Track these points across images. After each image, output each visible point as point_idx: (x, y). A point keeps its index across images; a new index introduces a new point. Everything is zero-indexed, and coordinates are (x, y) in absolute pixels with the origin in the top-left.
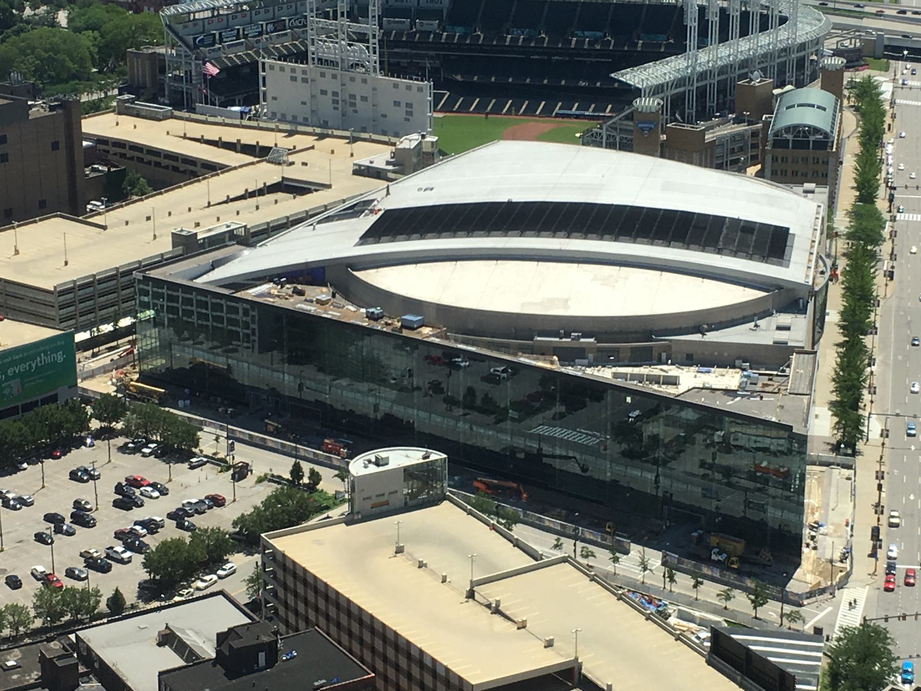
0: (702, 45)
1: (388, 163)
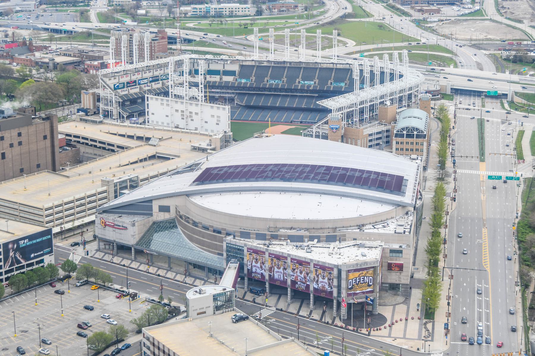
1: (208, 145)
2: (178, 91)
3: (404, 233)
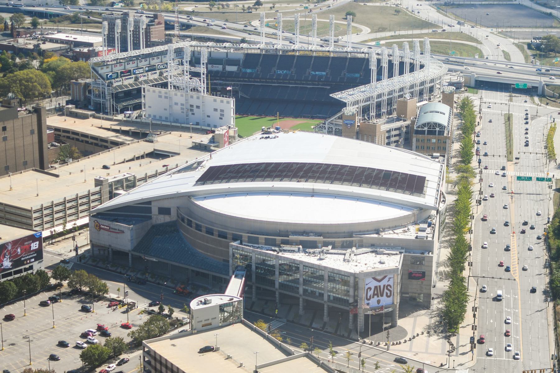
0: (379, 79)
3: (427, 238)
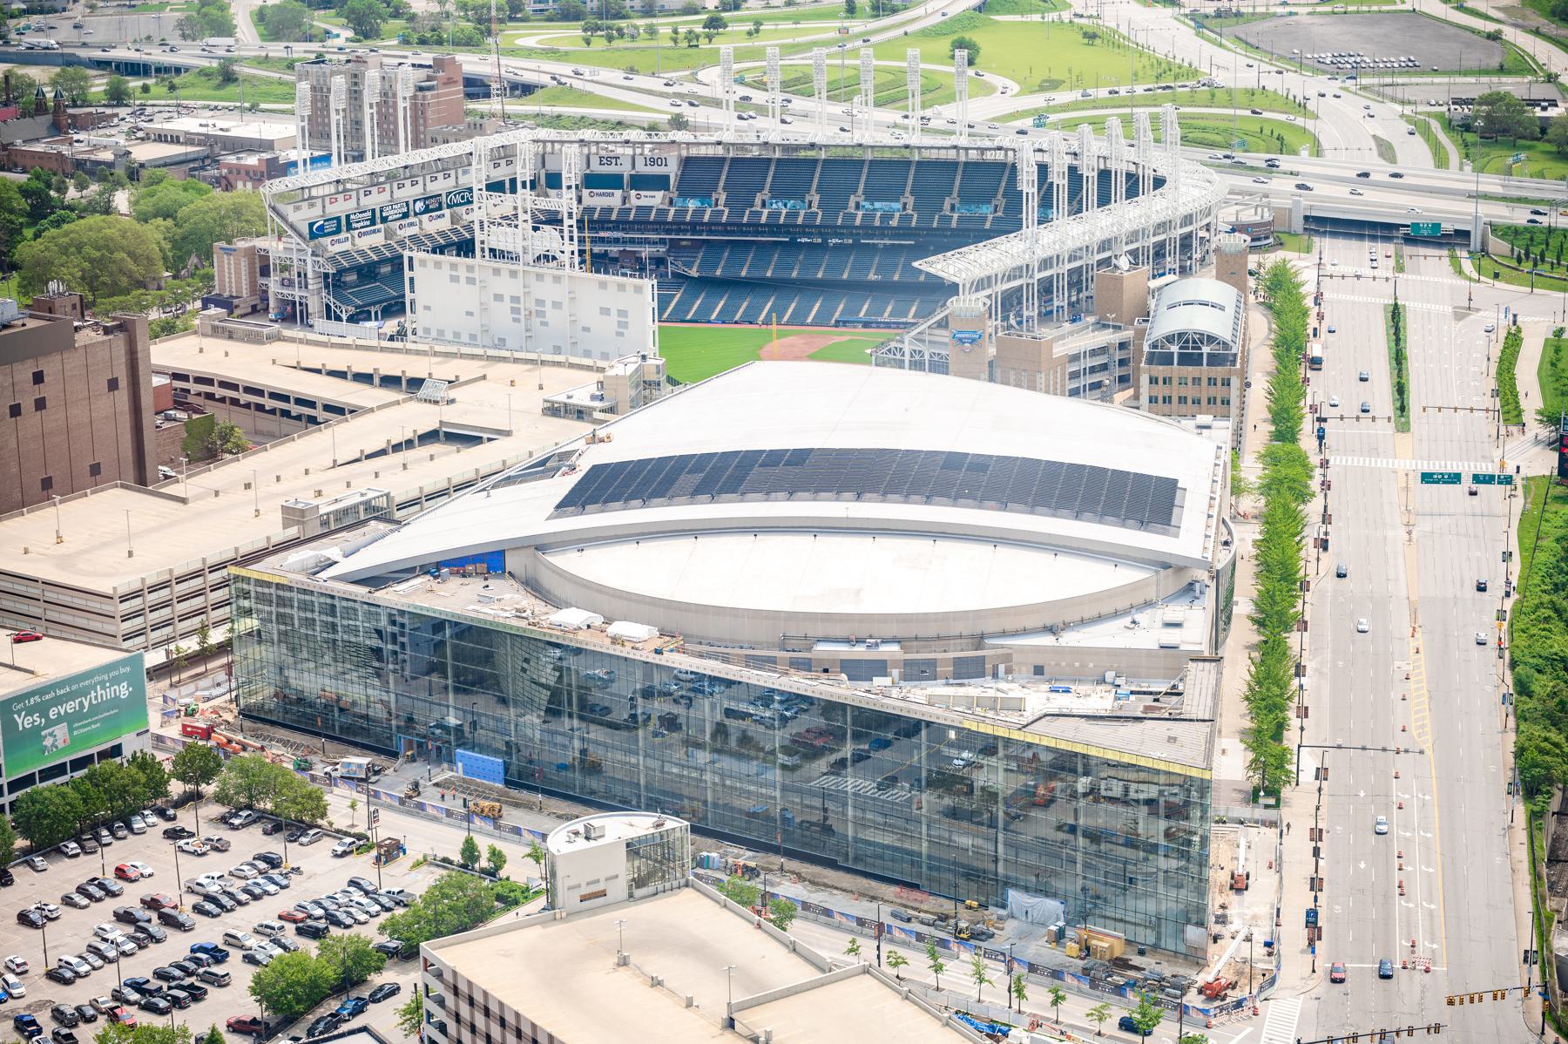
1: (593, 398)
2: (500, 238)
